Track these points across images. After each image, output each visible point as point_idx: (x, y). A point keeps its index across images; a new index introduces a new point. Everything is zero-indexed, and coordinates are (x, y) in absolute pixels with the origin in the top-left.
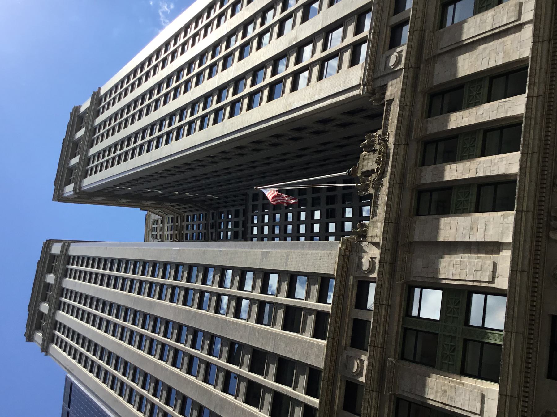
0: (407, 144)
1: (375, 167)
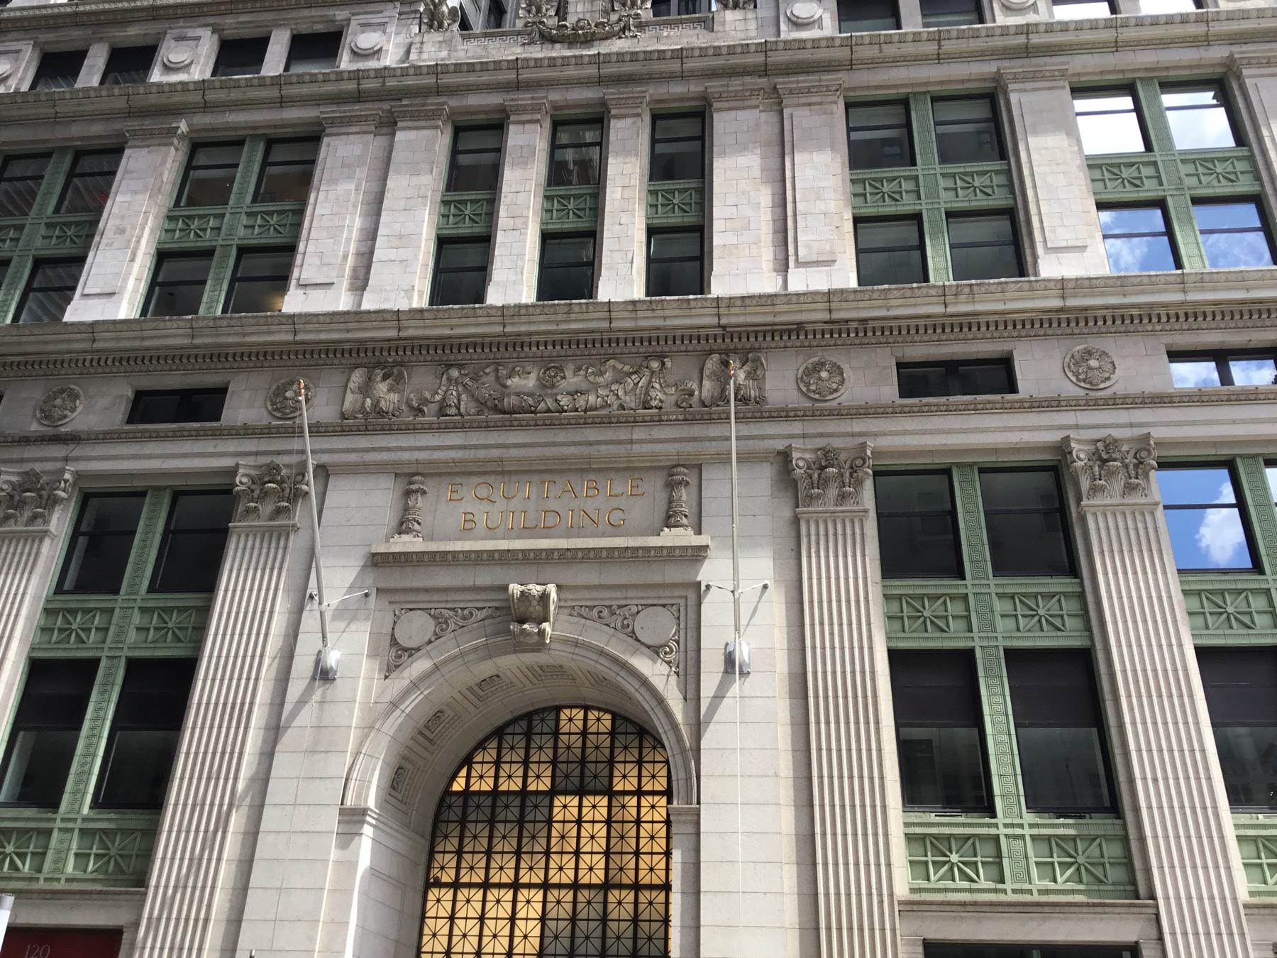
0: (600, 81)
1: (571, 20)
